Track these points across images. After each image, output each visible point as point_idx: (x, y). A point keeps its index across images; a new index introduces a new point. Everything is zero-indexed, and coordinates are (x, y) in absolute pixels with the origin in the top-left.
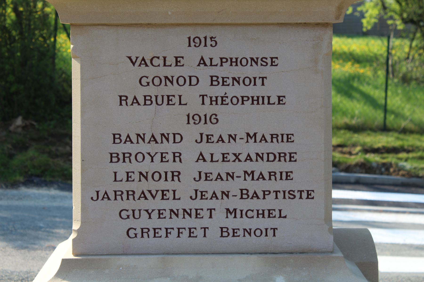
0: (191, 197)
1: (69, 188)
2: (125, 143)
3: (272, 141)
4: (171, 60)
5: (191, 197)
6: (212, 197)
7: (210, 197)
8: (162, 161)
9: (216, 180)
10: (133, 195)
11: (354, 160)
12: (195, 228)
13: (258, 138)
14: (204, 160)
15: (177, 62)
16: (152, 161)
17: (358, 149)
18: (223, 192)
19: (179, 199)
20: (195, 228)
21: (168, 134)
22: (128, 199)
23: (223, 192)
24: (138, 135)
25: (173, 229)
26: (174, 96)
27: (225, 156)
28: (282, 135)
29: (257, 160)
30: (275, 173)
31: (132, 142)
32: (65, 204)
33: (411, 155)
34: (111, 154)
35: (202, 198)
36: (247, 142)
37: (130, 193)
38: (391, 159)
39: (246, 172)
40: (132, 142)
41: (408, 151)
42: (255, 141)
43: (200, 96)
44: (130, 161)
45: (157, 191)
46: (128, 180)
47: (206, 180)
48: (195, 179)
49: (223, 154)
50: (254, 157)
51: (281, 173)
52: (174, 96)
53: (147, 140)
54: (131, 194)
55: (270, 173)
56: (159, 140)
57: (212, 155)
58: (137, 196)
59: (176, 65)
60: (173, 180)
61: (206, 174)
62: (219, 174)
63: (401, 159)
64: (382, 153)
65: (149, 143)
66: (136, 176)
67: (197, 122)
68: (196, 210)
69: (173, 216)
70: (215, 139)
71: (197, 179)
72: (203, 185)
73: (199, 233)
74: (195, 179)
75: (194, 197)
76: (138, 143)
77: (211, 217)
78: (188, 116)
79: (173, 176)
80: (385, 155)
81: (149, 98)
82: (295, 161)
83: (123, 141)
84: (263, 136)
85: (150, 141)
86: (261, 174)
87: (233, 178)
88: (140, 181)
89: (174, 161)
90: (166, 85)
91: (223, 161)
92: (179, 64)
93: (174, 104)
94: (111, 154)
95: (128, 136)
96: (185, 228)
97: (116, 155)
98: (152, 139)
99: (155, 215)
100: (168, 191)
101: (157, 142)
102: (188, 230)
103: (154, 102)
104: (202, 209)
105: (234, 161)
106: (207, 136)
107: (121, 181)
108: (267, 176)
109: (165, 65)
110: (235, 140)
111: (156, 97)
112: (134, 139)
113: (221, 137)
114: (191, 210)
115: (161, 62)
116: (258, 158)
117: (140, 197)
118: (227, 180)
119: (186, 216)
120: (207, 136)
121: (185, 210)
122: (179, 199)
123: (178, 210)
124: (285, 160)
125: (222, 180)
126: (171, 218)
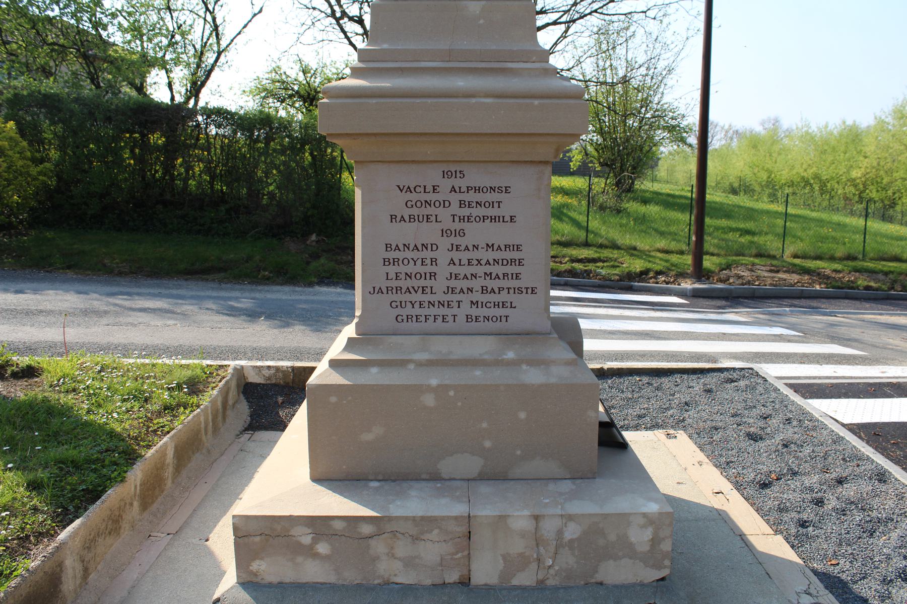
0: (444, 292)
2: (395, 251)
5: (444, 292)
7: (458, 292)
8: (422, 265)
10: (401, 290)
14: (455, 264)
16: (415, 265)
18: (468, 289)
21: (427, 244)
22: (397, 293)
23: (468, 289)
24: (405, 245)
26: (432, 215)
29: (494, 265)
31: (400, 250)
34: (384, 259)
36: (487, 250)
37: (399, 289)
39: (485, 273)
40: (400, 250)
44: (398, 265)
45: (419, 287)
46: (396, 279)
49: (469, 260)
50: (492, 262)
51: (512, 274)
52: (432, 215)
54: (398, 289)
55: (504, 274)
56: (420, 249)
57: (460, 260)
58: (403, 291)
60: (430, 279)
61: (456, 274)
62: (465, 275)
66: (403, 276)
67: (449, 235)
68: (448, 302)
69: (431, 306)
71: (449, 278)
72: (453, 283)
78: (442, 230)
79: (431, 276)
82: (523, 265)
83: (393, 250)
86: (497, 275)
87: (476, 278)
89: (432, 264)
91: (469, 265)
95: (397, 246)
99: (417, 305)
100: (427, 287)
101: (418, 251)
105: (477, 265)
106: (457, 246)
108: (501, 277)
110: (477, 249)
113: (467, 246)
114: (444, 302)
116: (495, 263)
118: (472, 279)
119: (441, 306)
120: (457, 246)
121: (439, 302)
124: (515, 265)
125: (468, 279)
126: (429, 307)
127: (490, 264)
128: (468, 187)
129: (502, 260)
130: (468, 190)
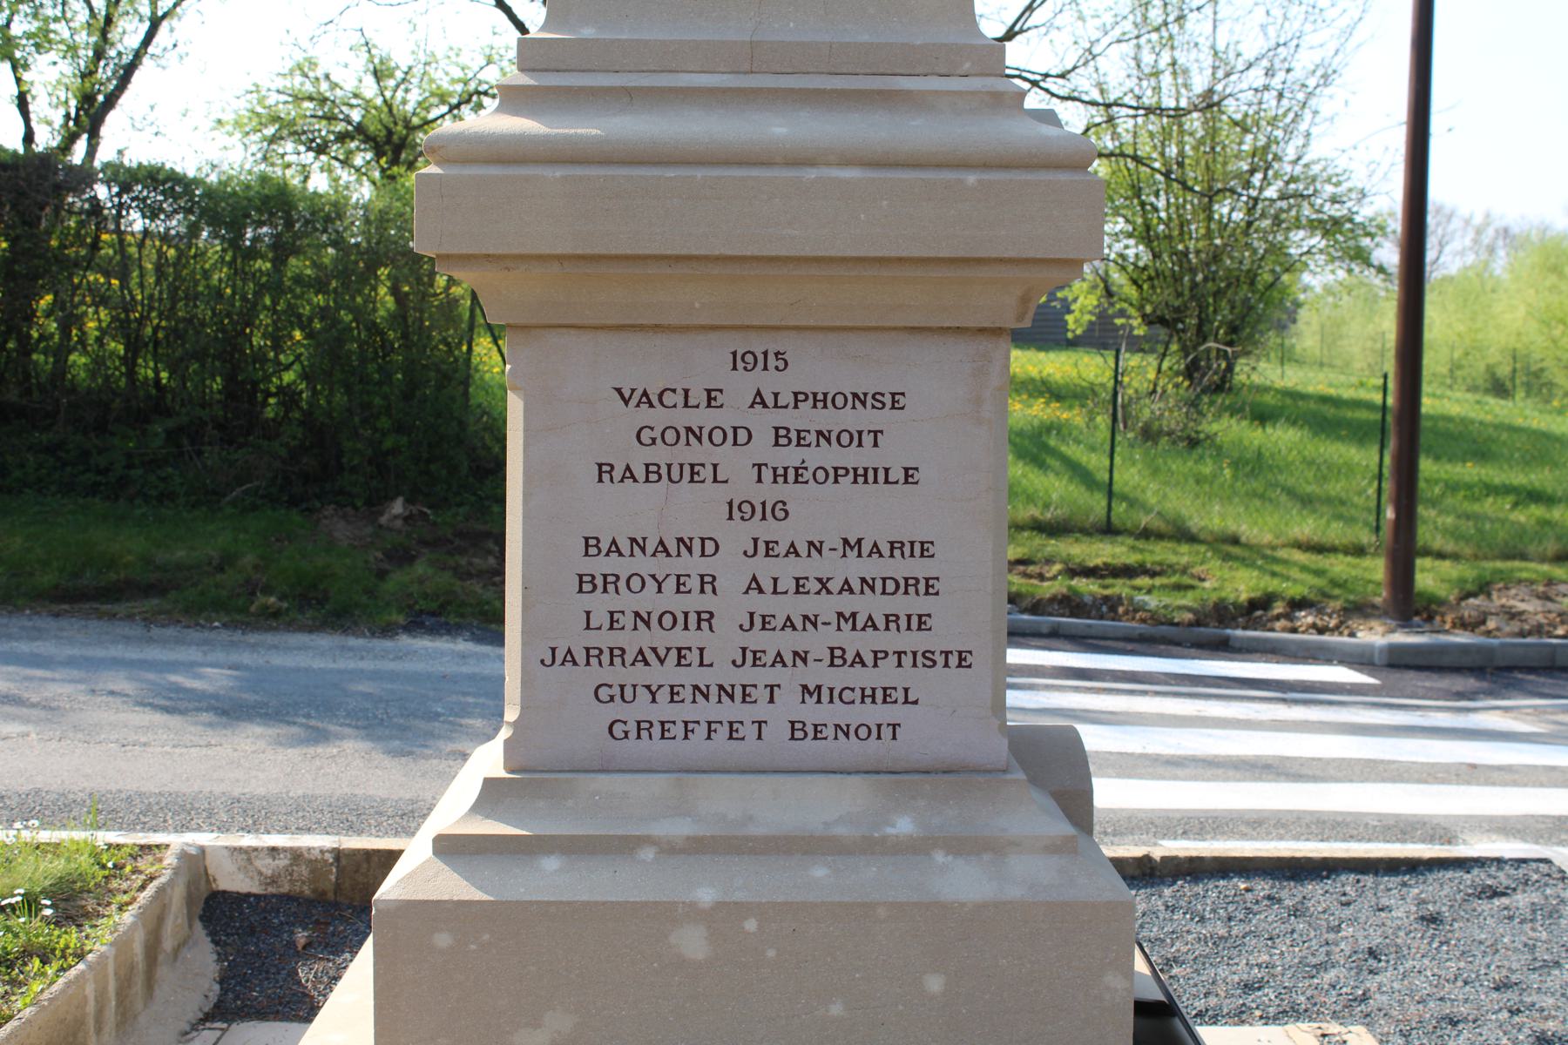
0: (734, 662)
1: (499, 639)
2: (607, 555)
3: (892, 556)
4: (698, 396)
5: (734, 662)
6: (775, 662)
7: (770, 663)
8: (678, 591)
9: (783, 629)
10: (622, 656)
11: (1048, 589)
12: (742, 723)
13: (866, 548)
14: (761, 591)
15: (710, 399)
16: (660, 591)
17: (1057, 567)
18: (796, 654)
19: (711, 665)
20: (742, 723)
21: (691, 539)
22: (612, 663)
23: (796, 654)
24: (633, 540)
25: (698, 722)
26: (703, 465)
27: (801, 582)
28: (912, 543)
29: (862, 592)
30: (898, 617)
31: (621, 554)
32: (487, 669)
33: (1158, 581)
35: (754, 665)
36: (844, 555)
37: (617, 652)
38: (1120, 587)
39: (840, 615)
40: (621, 554)
41: (1153, 574)
42: (860, 555)
43: (754, 465)
44: (617, 591)
45: (668, 649)
46: (611, 628)
47: (763, 628)
48: (741, 626)
49: (797, 580)
50: (856, 585)
51: (909, 617)
52: (703, 465)
53: (650, 549)
54: (616, 654)
55: (887, 616)
56: (673, 551)
57: (775, 580)
58: (629, 658)
59: (709, 406)
60: (699, 628)
61: (764, 617)
62: (788, 618)
63: (1139, 589)
64: (1102, 577)
65: (654, 555)
66: (627, 620)
67: (747, 517)
68: (744, 687)
69: (699, 697)
70: (781, 549)
71: (747, 626)
72: (756, 639)
73: (749, 731)
74: (741, 626)
75: (739, 662)
76: (632, 555)
77: (772, 701)
78: (730, 504)
79: (699, 620)
80: (1109, 581)
81: (654, 468)
82: (937, 594)
83: (604, 552)
84: (875, 545)
85: (656, 551)
86: (870, 618)
87: (815, 625)
88: (635, 628)
89: (702, 591)
90: (688, 444)
91: (797, 592)
92: (713, 403)
93: (703, 482)
94: (581, 576)
95: (614, 542)
96: (721, 723)
97: (589, 578)
98: (660, 549)
99: (663, 696)
100: (689, 649)
101: (669, 555)
102: (727, 726)
103: (665, 476)
104: (755, 686)
105: (818, 593)
106: (767, 543)
107: (600, 628)
108: (881, 623)
109: (686, 405)
110: (820, 552)
111: (669, 466)
112: (625, 548)
113: (792, 545)
114: (733, 686)
115: (680, 399)
116: (865, 587)
117: (635, 660)
118: (804, 629)
119: (725, 698)
120: (767, 543)
121: (721, 687)
122: (711, 665)
123: (708, 687)
124: (917, 593)
125: (794, 629)
127: (851, 591)
128: (796, 394)
129: (884, 580)
130: (796, 401)
